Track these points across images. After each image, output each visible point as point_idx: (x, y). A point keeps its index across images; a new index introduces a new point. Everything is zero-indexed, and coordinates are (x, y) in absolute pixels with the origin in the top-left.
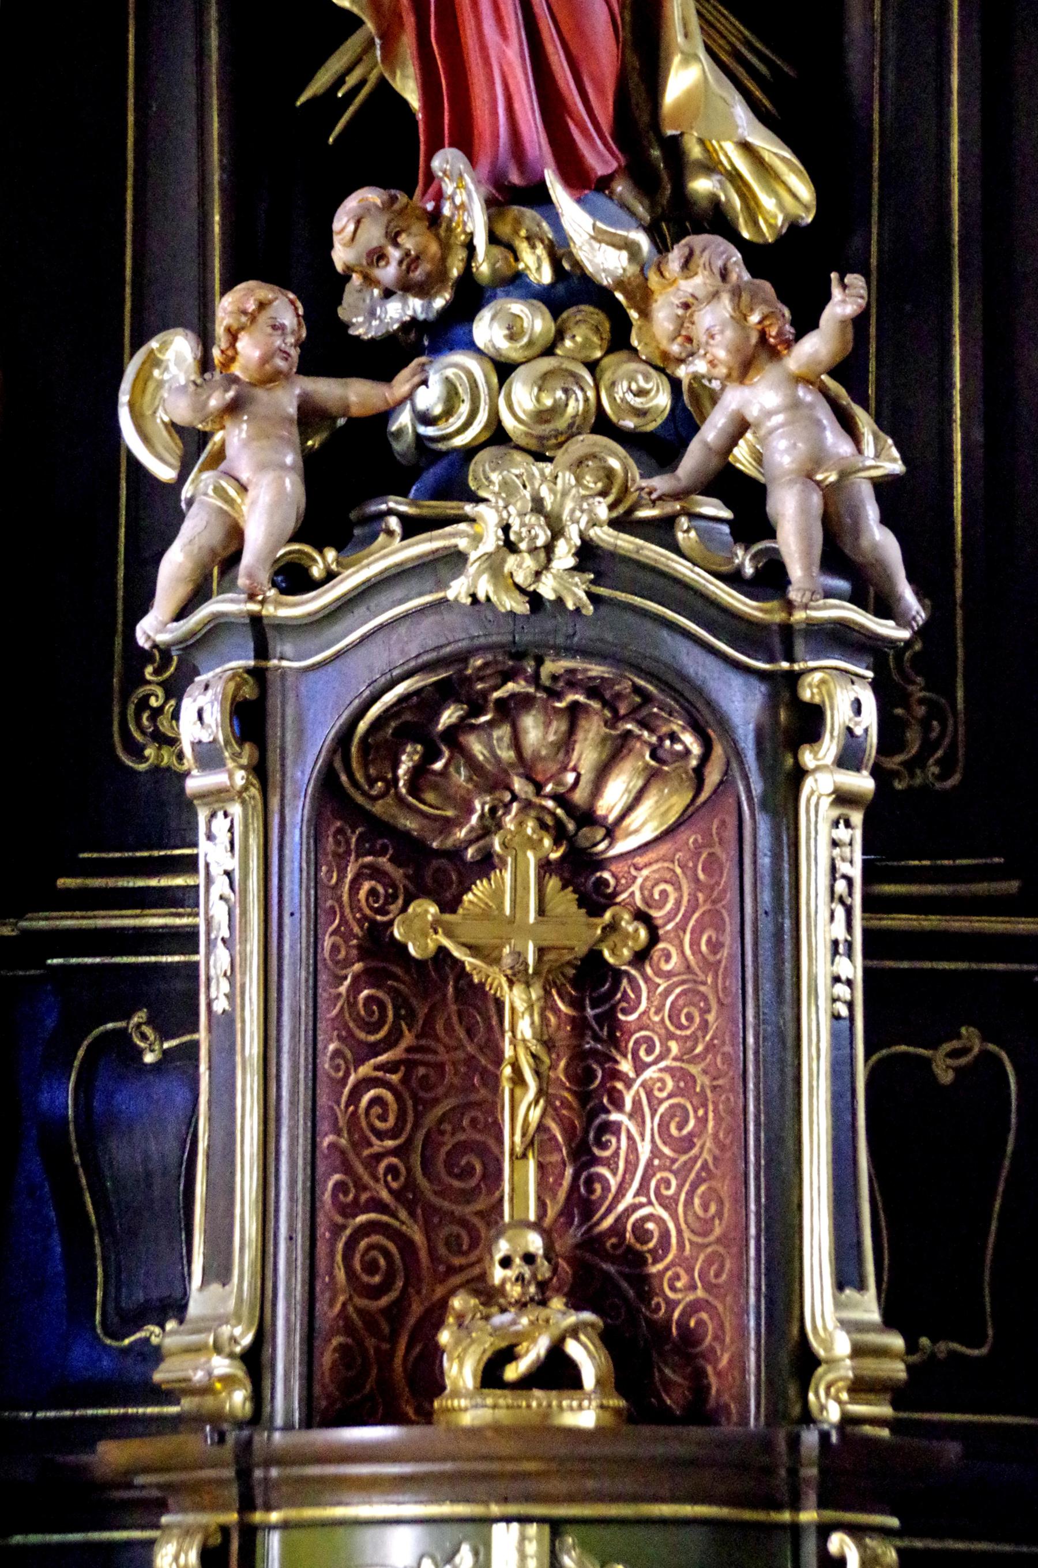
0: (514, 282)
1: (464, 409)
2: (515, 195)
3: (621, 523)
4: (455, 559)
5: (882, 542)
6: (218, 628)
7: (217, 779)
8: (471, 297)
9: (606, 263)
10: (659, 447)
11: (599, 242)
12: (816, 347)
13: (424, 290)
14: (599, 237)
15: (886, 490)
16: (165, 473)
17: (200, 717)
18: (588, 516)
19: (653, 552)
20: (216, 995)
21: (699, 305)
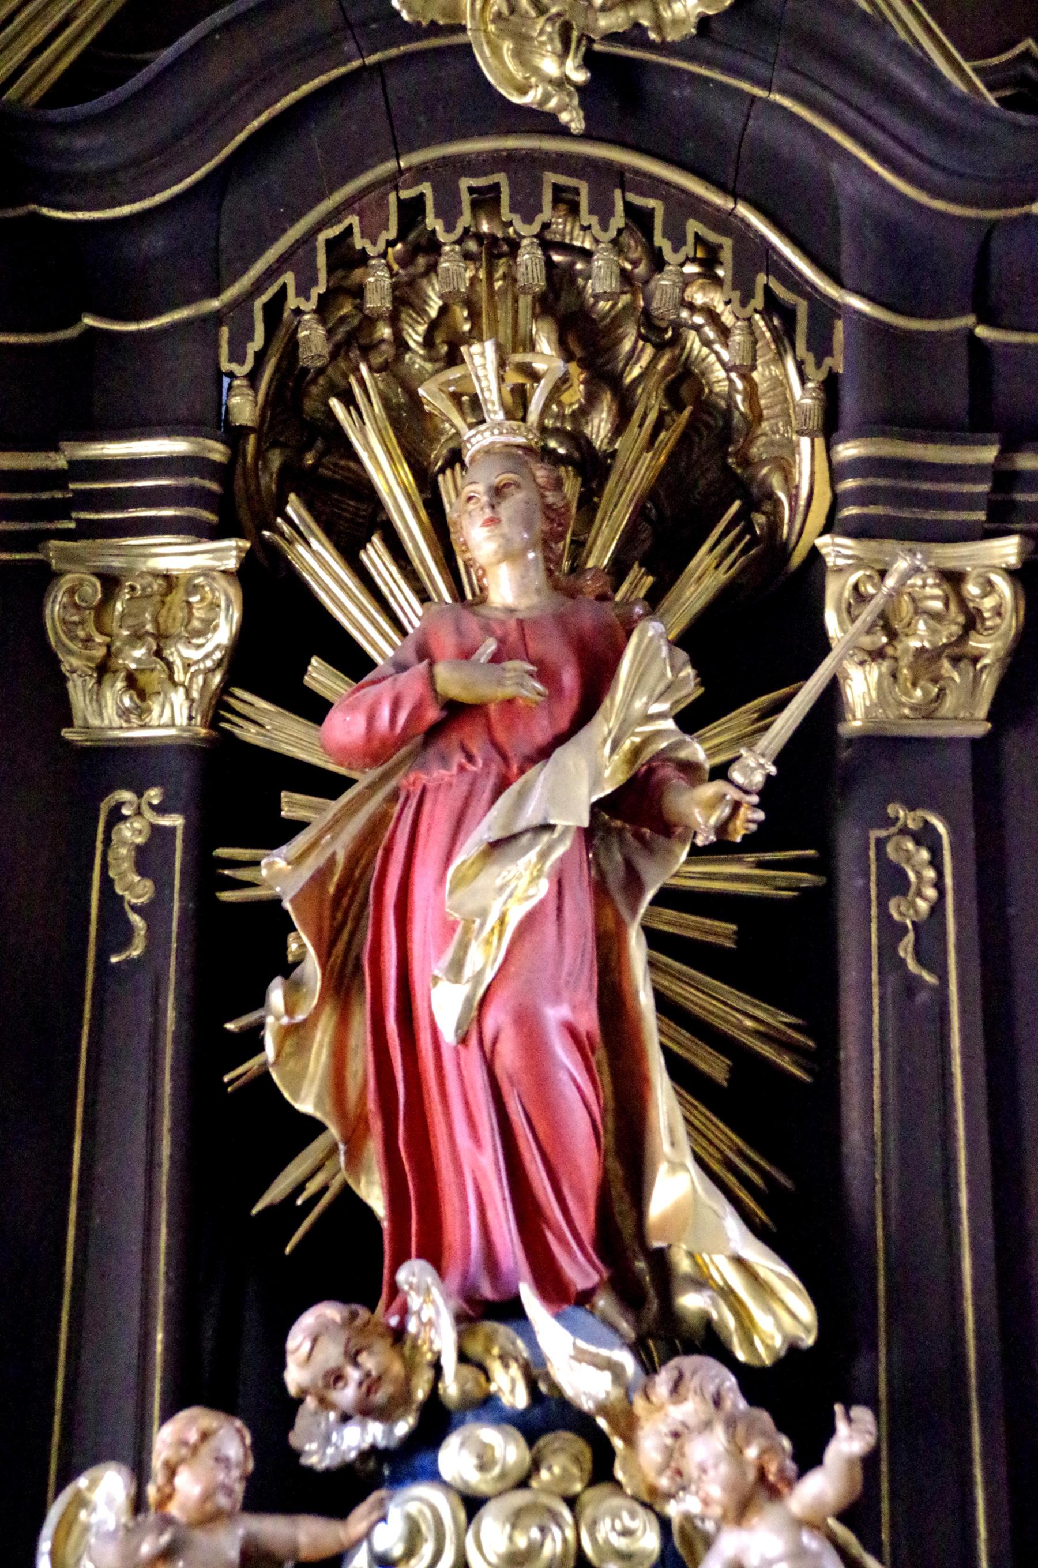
1: (427, 1550)
2: (488, 1309)
8: (436, 1422)
9: (585, 1385)
11: (581, 1361)
12: (822, 1487)
13: (385, 1414)
14: (580, 1356)
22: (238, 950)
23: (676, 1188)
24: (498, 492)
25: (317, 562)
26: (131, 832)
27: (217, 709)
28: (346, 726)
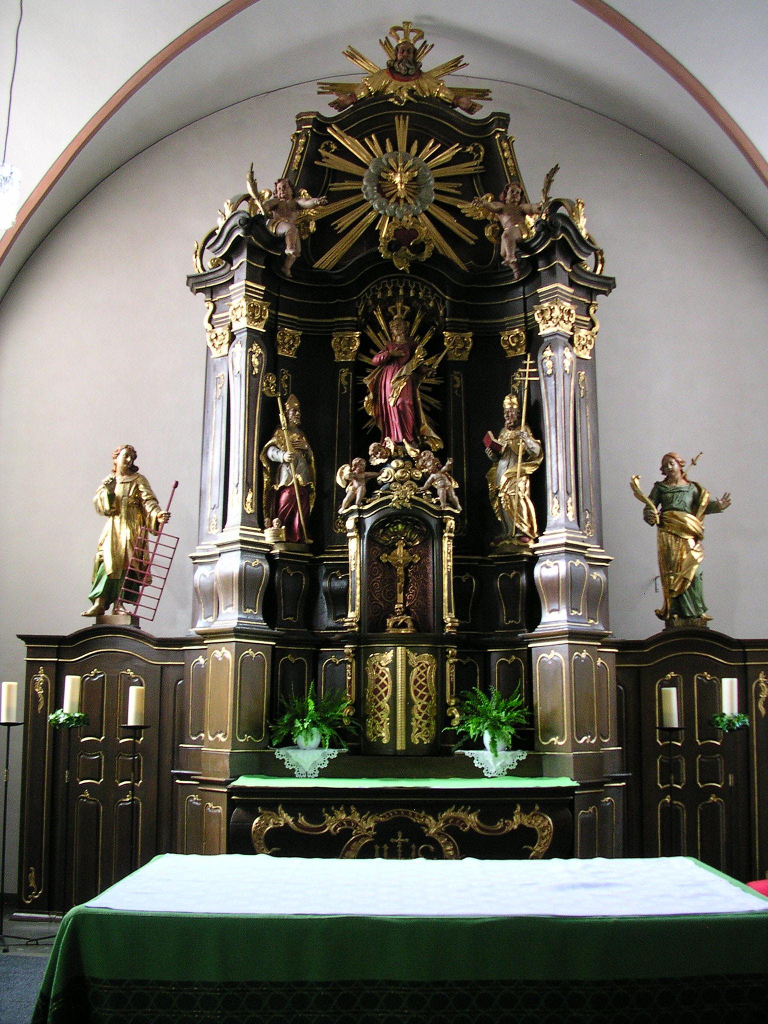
0: (398, 457)
3: (415, 495)
4: (389, 501)
5: (456, 498)
6: (352, 512)
7: (354, 534)
9: (413, 454)
10: (421, 483)
15: (455, 490)
16: (343, 486)
17: (350, 524)
18: (411, 494)
19: (420, 500)
20: (352, 568)
21: (428, 460)
22: (362, 391)
23: (426, 426)
24: (398, 325)
25: (371, 333)
26: (344, 375)
27: (357, 357)
28: (376, 359)
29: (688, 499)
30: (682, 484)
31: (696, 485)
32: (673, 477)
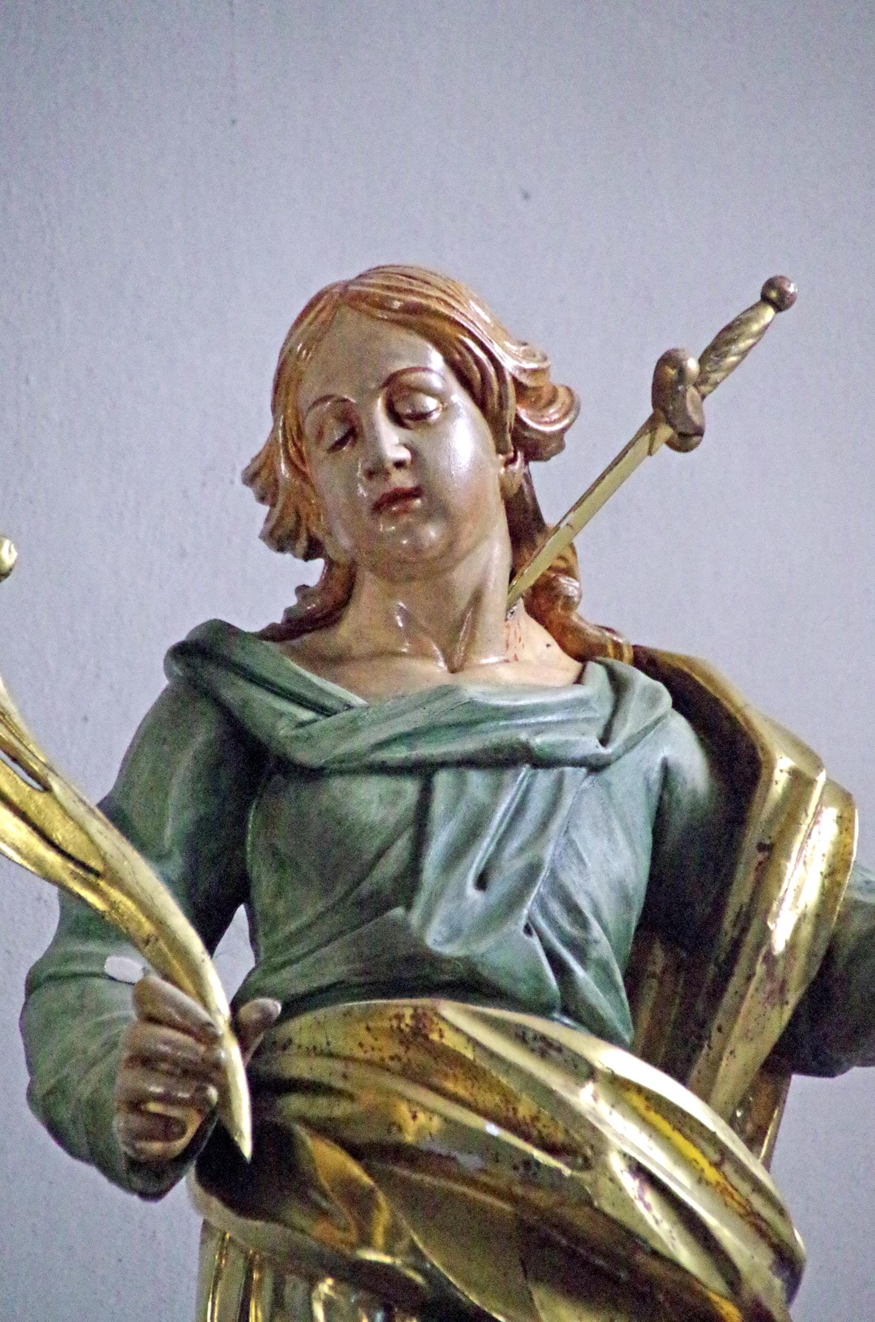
29: (606, 863)
30: (520, 669)
31: (695, 699)
32: (426, 571)
